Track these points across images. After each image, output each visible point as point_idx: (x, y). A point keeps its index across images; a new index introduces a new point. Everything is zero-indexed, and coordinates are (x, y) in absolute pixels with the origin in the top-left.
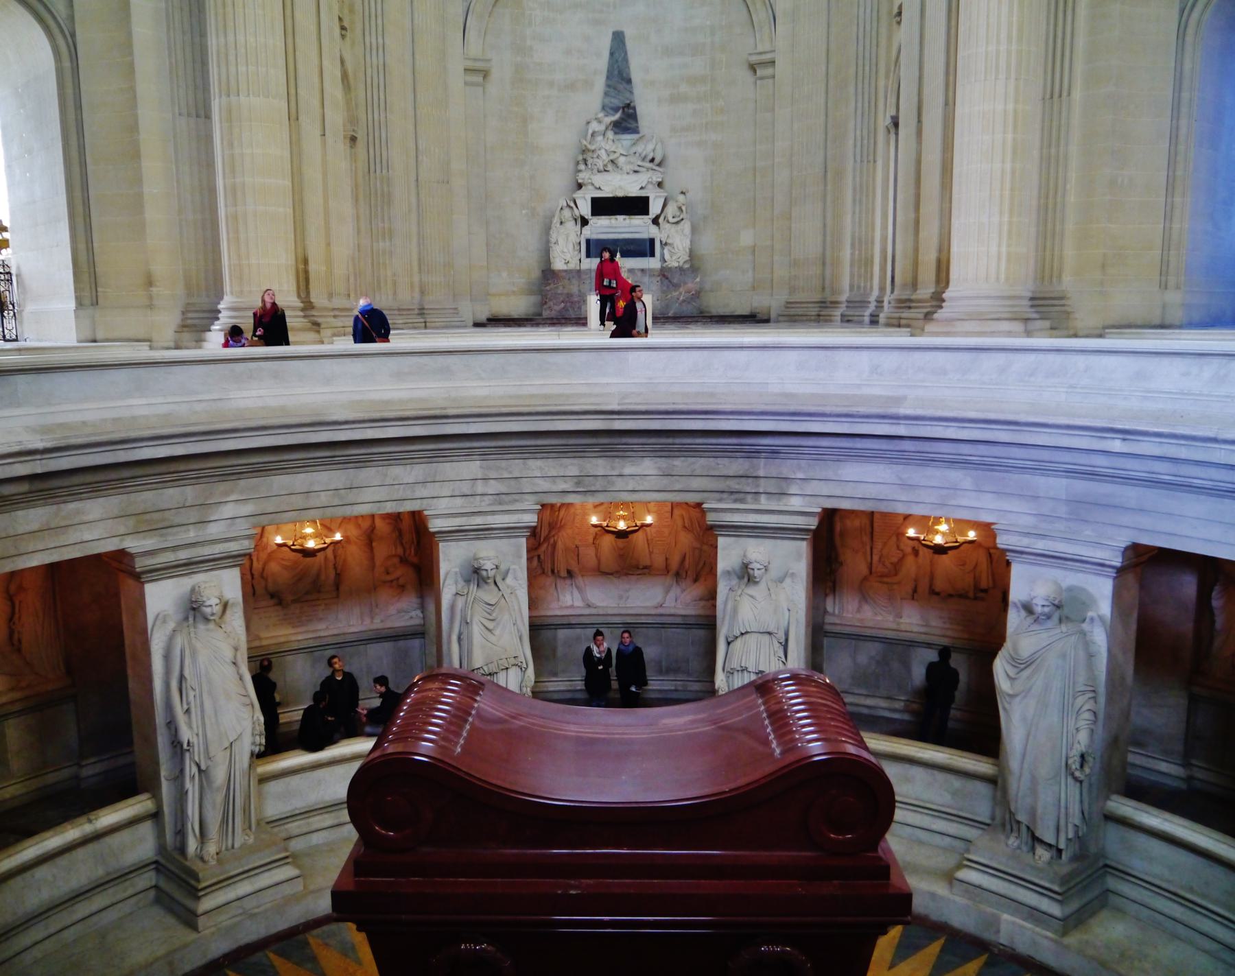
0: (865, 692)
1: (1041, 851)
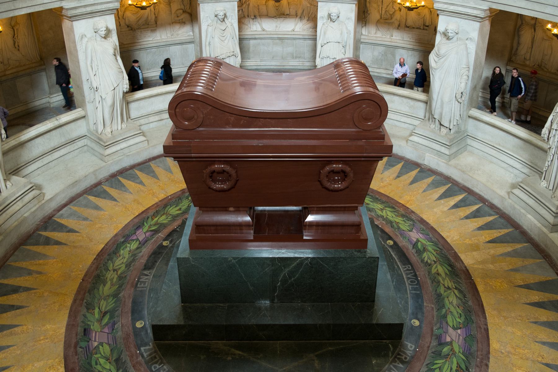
0: (376, 66)
1: (443, 129)
